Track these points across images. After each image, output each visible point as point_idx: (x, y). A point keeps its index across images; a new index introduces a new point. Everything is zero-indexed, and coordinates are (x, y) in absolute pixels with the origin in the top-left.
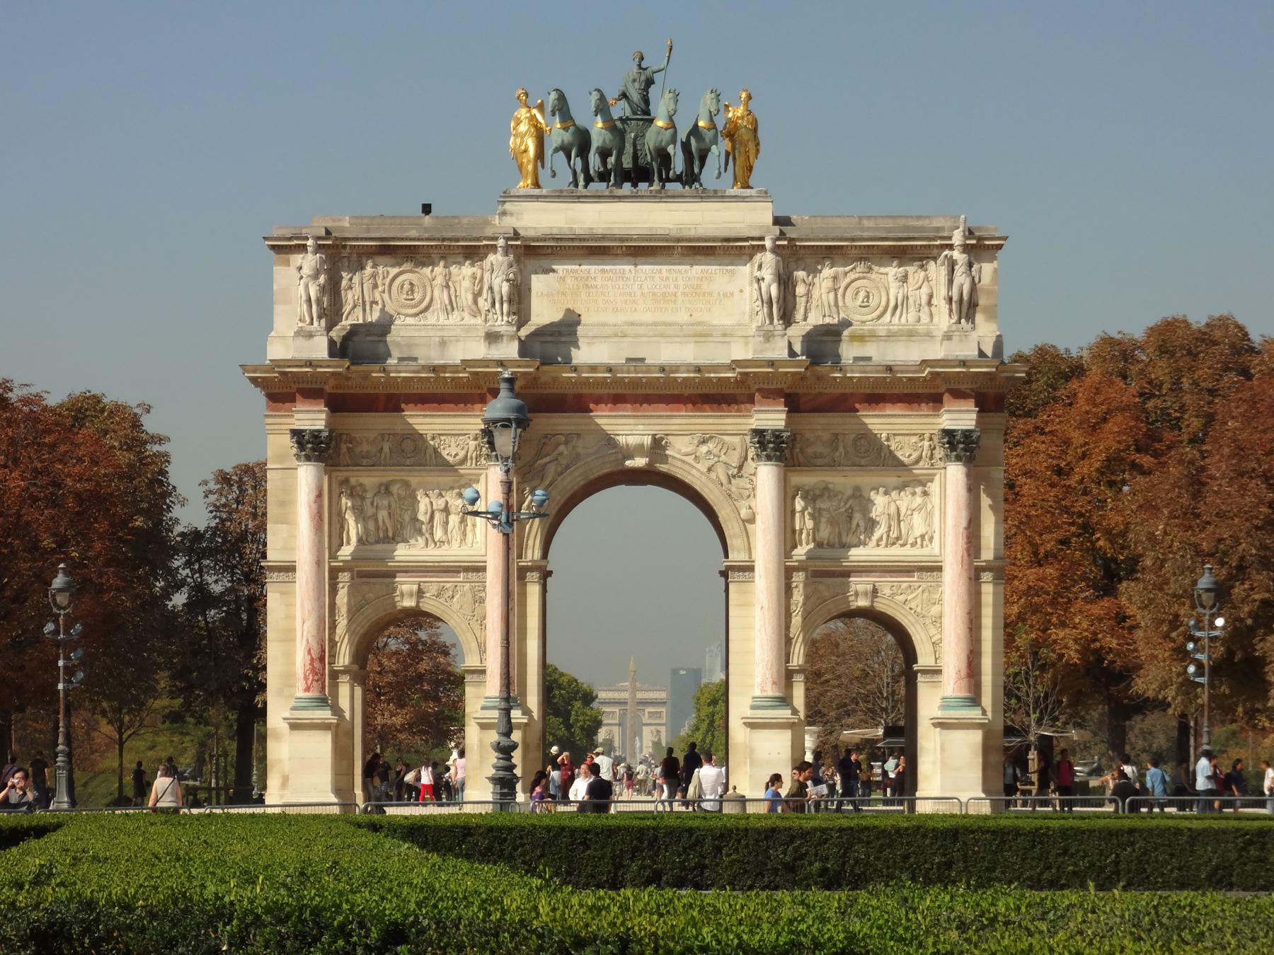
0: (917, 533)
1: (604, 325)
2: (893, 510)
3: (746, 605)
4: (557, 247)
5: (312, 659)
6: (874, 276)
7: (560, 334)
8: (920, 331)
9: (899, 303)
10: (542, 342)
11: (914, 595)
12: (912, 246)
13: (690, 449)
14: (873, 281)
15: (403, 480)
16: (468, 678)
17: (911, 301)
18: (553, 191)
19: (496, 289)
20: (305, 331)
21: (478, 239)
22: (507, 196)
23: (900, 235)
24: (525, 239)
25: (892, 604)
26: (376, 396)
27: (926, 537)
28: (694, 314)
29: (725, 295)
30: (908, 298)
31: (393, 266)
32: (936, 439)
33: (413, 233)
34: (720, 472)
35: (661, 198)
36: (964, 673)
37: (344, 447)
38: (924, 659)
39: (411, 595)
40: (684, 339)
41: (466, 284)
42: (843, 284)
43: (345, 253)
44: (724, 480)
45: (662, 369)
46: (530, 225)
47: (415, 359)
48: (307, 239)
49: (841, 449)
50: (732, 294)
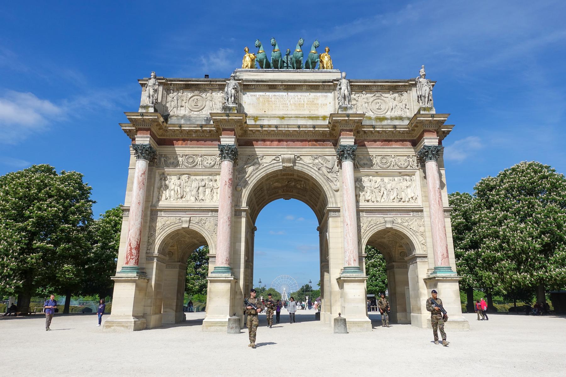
0: (410, 197)
1: (275, 114)
5: (131, 248)
6: (383, 98)
9: (394, 107)
13: (311, 161)
16: (210, 260)
17: (398, 106)
19: (229, 92)
25: (402, 227)
27: (414, 198)
34: (324, 170)
36: (445, 256)
37: (163, 159)
38: (418, 251)
39: (186, 222)
41: (220, 100)
43: (172, 87)
45: (299, 127)
50: (326, 104)
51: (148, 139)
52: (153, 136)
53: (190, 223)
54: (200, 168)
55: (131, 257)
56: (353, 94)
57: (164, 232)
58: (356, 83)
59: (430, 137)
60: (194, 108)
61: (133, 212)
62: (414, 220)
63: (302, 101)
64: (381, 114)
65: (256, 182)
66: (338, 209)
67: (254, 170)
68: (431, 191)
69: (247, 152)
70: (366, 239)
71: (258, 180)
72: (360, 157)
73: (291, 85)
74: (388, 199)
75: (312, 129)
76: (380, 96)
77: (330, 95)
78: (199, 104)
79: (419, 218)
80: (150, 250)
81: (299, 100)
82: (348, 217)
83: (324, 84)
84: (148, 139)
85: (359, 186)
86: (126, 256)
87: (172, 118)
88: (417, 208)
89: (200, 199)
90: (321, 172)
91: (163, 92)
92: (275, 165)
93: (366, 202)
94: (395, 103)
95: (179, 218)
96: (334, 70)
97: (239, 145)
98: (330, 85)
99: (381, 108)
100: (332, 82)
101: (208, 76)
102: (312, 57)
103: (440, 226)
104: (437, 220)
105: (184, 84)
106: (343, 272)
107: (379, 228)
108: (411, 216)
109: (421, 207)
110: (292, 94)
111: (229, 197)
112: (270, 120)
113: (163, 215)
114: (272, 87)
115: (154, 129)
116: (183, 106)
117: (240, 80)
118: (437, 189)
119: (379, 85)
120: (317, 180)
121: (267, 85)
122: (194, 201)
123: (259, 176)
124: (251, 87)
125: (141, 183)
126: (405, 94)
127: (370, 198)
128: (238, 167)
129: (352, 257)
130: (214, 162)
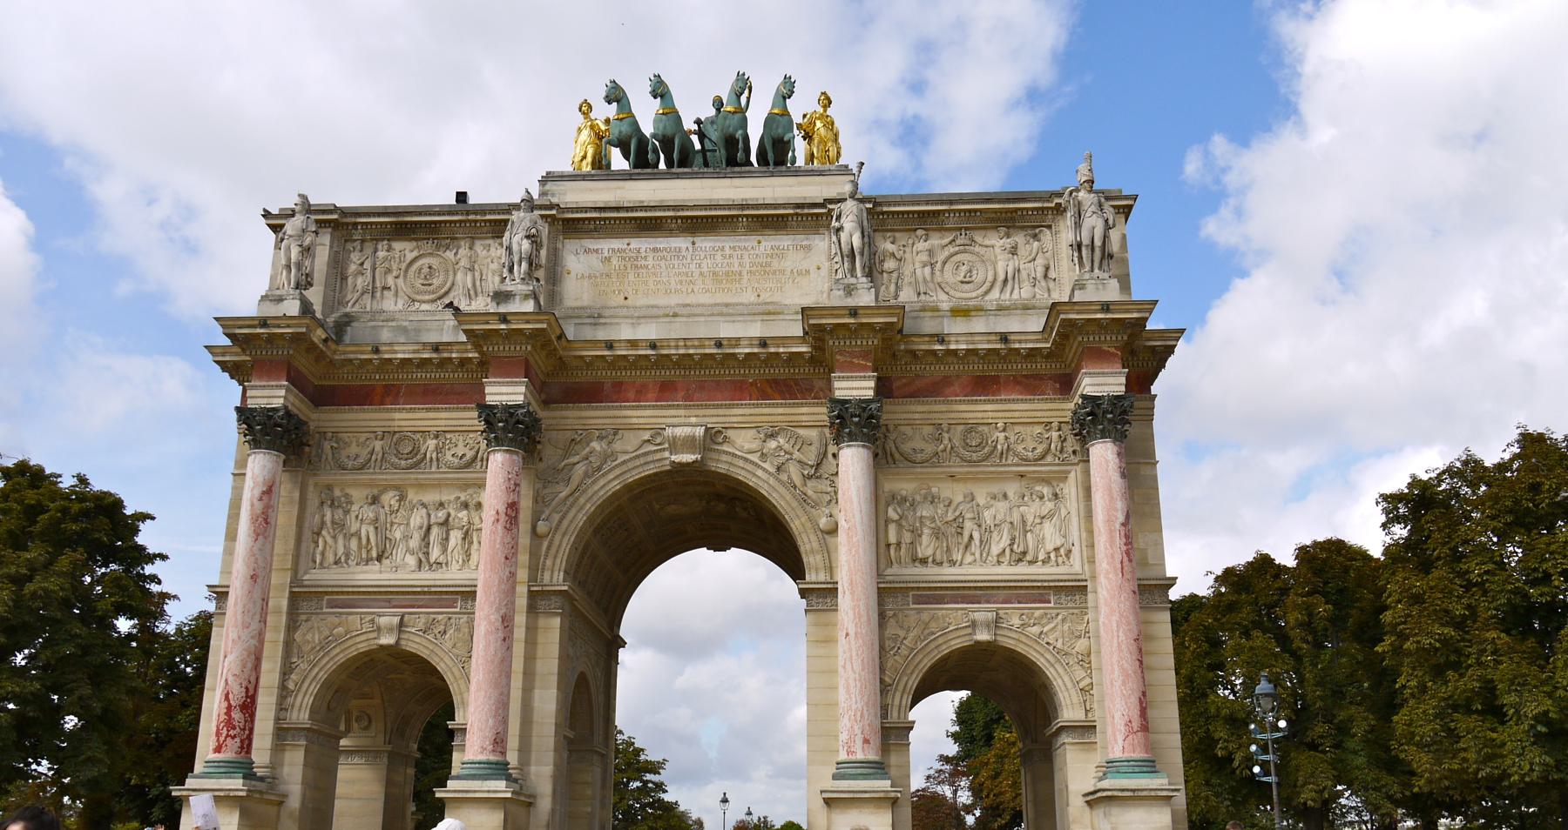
0: (1050, 547)
2: (1016, 518)
3: (829, 641)
4: (600, 219)
5: (229, 708)
6: (977, 249)
7: (600, 316)
9: (1010, 276)
11: (1051, 625)
13: (755, 446)
14: (977, 254)
15: (396, 488)
17: (1024, 274)
19: (515, 247)
25: (1023, 639)
26: (372, 389)
27: (1062, 551)
29: (800, 273)
30: (1019, 270)
32: (1066, 428)
34: (794, 471)
37: (327, 446)
38: (1069, 711)
39: (390, 630)
40: (751, 318)
42: (941, 257)
44: (797, 480)
45: (719, 344)
49: (946, 442)
50: (808, 272)
51: (283, 392)
52: (296, 380)
53: (400, 631)
54: (433, 470)
55: (228, 731)
56: (888, 241)
57: (327, 659)
58: (895, 205)
60: (418, 293)
61: (236, 604)
62: (1060, 617)
63: (736, 265)
64: (968, 295)
65: (593, 509)
66: (829, 586)
67: (586, 475)
68: (1100, 531)
69: (569, 421)
70: (914, 676)
71: (599, 503)
72: (902, 428)
73: (702, 217)
74: (984, 555)
75: (756, 350)
76: (968, 242)
77: (821, 244)
78: (434, 281)
79: (1076, 611)
80: (286, 710)
81: (726, 261)
82: (851, 613)
83: (799, 211)
84: (283, 392)
85: (896, 517)
86: (215, 729)
87: (353, 324)
88: (1069, 581)
89: (432, 561)
90: (784, 477)
91: (331, 247)
92: (650, 458)
93: (917, 564)
95: (370, 617)
97: (546, 403)
101: (464, 194)
103: (1122, 637)
104: (1114, 618)
105: (391, 223)
106: (835, 777)
107: (953, 643)
108: (1052, 605)
109: (1083, 577)
110: (706, 243)
111: (507, 558)
112: (639, 324)
113: (325, 610)
114: (648, 223)
115: (303, 363)
117: (551, 206)
118: (1118, 526)
119: (965, 211)
120: (774, 502)
121: (631, 219)
122: (413, 568)
123: (602, 493)
125: (260, 519)
126: (1046, 236)
127: (929, 552)
128: (541, 466)
129: (858, 732)
130: (472, 453)
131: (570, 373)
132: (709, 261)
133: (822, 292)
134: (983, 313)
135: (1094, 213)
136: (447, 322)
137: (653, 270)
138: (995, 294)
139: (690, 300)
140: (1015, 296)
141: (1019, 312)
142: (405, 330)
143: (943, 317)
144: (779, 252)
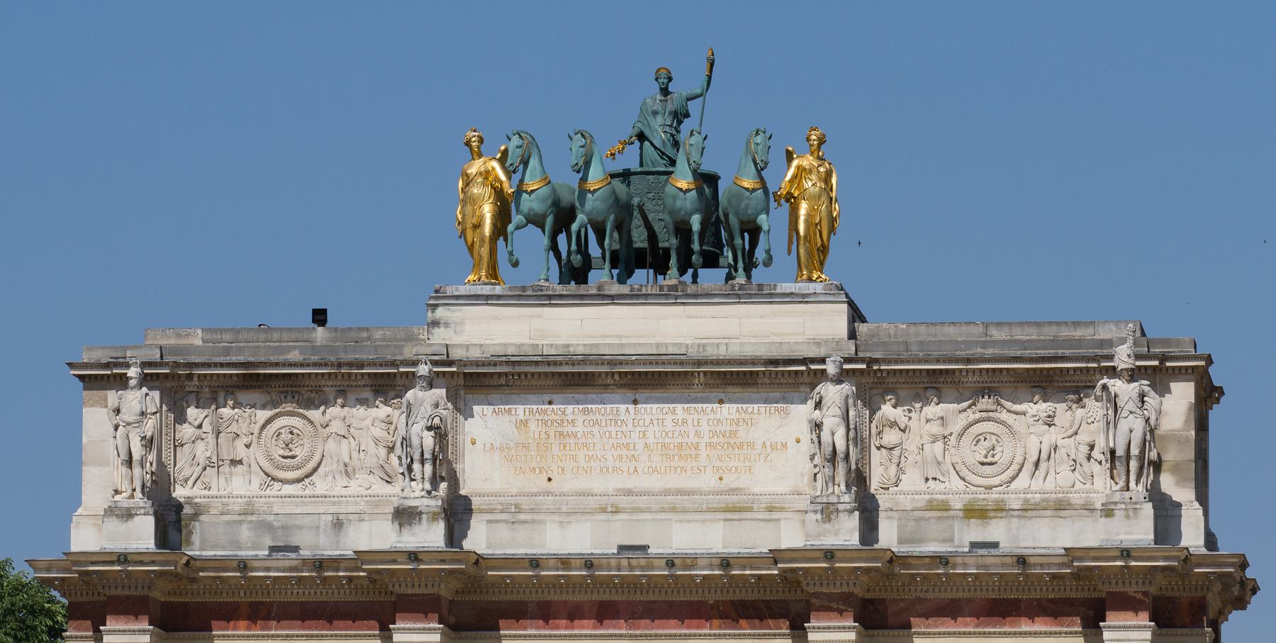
6: (1004, 416)
7: (519, 510)
8: (1072, 502)
9: (1044, 456)
10: (489, 522)
12: (1061, 369)
14: (1003, 423)
17: (1062, 452)
18: (510, 288)
19: (415, 442)
20: (120, 509)
21: (393, 364)
22: (439, 297)
23: (1043, 353)
24: (462, 363)
28: (724, 476)
29: (774, 447)
31: (263, 407)
33: (295, 356)
35: (676, 297)
40: (710, 516)
41: (378, 432)
43: (192, 386)
45: (671, 563)
46: (476, 341)
47: (296, 549)
48: (128, 366)
50: (784, 445)
59: (1122, 623)
60: (278, 467)
63: (692, 435)
76: (994, 407)
78: (297, 451)
81: (678, 429)
87: (203, 518)
94: (1052, 436)
96: (818, 288)
98: (796, 372)
99: (996, 458)
100: (804, 361)
102: (743, 206)
116: (240, 462)
119: (987, 370)
121: (553, 374)
124: (495, 381)
131: (485, 590)
132: (656, 428)
133: (802, 475)
134: (1004, 514)
135: (1131, 412)
136: (323, 517)
137: (583, 440)
138: (1023, 481)
139: (630, 483)
140: (1050, 485)
141: (1049, 513)
142: (268, 527)
143: (953, 518)
144: (747, 417)
